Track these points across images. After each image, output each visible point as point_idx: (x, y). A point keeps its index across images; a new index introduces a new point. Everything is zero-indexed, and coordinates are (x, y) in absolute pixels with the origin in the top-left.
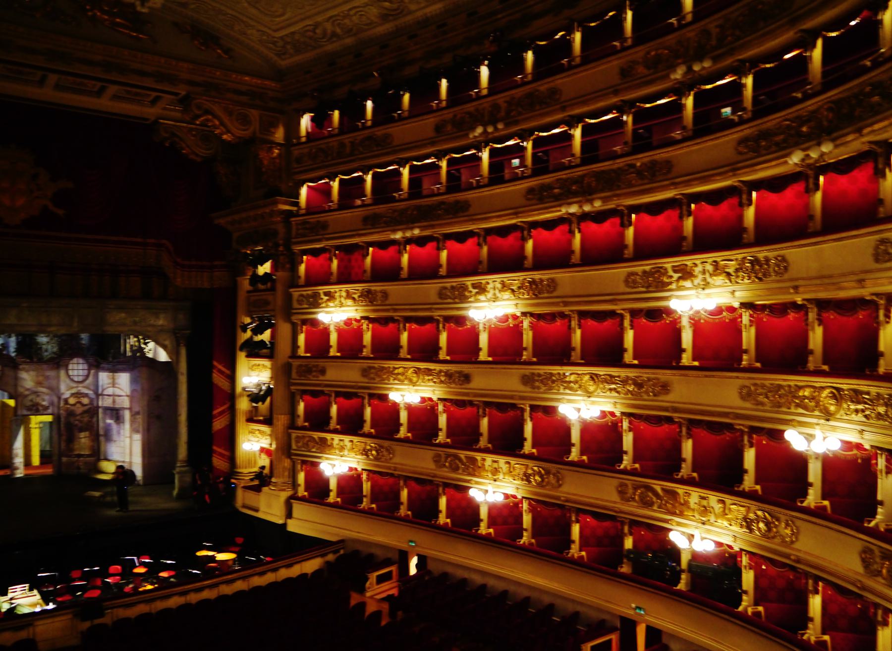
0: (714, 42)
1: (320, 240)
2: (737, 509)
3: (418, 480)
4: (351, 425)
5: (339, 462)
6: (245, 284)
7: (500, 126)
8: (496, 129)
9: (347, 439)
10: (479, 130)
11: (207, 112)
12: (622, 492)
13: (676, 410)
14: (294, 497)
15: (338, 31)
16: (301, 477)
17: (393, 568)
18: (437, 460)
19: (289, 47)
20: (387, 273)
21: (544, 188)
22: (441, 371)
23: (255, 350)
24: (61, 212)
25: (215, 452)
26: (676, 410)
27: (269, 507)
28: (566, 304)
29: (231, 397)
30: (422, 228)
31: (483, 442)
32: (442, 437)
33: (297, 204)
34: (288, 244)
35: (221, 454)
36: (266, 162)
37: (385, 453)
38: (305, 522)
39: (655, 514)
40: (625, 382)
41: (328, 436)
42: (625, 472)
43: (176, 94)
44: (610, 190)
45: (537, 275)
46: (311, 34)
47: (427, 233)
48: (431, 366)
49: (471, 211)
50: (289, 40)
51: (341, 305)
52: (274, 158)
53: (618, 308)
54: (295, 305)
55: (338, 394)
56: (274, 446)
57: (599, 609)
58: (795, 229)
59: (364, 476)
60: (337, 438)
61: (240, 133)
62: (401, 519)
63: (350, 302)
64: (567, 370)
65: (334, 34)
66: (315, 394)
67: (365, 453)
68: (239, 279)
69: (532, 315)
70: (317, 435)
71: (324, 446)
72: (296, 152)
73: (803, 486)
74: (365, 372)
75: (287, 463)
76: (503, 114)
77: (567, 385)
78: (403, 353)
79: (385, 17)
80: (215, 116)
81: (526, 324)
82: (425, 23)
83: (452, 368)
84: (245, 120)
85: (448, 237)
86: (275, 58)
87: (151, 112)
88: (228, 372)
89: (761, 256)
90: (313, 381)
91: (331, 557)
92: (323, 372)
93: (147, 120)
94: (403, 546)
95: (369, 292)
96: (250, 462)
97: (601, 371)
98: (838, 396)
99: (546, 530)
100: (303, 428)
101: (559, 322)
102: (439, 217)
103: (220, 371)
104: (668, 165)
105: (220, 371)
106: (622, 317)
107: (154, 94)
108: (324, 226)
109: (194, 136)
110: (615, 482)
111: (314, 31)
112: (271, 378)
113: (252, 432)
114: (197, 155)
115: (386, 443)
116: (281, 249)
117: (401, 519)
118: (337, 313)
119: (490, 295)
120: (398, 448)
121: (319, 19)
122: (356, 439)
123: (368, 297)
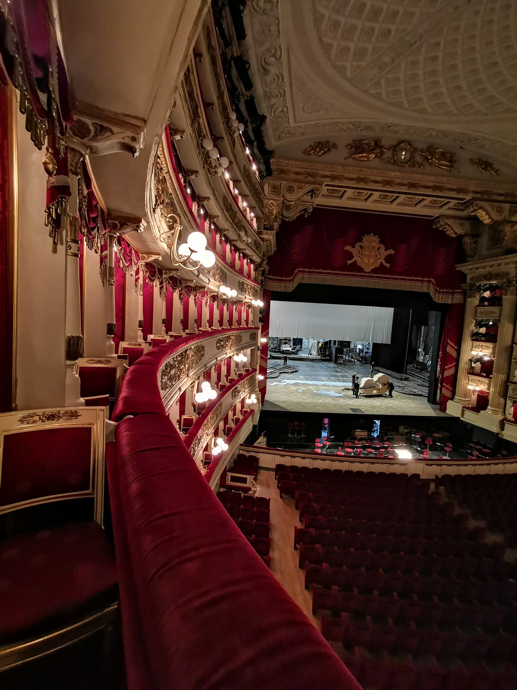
11: (481, 208)
14: (505, 419)
16: (510, 410)
23: (476, 337)
24: (388, 265)
25: (445, 387)
27: (487, 420)
29: (457, 360)
36: (508, 234)
43: (464, 199)
52: (514, 231)
56: (492, 390)
75: (502, 400)
84: (500, 211)
87: (434, 212)
88: (456, 348)
93: (432, 217)
96: (466, 394)
103: (452, 346)
105: (452, 346)
107: (447, 200)
109: (456, 223)
112: (493, 353)
113: (473, 381)
116: (514, 282)
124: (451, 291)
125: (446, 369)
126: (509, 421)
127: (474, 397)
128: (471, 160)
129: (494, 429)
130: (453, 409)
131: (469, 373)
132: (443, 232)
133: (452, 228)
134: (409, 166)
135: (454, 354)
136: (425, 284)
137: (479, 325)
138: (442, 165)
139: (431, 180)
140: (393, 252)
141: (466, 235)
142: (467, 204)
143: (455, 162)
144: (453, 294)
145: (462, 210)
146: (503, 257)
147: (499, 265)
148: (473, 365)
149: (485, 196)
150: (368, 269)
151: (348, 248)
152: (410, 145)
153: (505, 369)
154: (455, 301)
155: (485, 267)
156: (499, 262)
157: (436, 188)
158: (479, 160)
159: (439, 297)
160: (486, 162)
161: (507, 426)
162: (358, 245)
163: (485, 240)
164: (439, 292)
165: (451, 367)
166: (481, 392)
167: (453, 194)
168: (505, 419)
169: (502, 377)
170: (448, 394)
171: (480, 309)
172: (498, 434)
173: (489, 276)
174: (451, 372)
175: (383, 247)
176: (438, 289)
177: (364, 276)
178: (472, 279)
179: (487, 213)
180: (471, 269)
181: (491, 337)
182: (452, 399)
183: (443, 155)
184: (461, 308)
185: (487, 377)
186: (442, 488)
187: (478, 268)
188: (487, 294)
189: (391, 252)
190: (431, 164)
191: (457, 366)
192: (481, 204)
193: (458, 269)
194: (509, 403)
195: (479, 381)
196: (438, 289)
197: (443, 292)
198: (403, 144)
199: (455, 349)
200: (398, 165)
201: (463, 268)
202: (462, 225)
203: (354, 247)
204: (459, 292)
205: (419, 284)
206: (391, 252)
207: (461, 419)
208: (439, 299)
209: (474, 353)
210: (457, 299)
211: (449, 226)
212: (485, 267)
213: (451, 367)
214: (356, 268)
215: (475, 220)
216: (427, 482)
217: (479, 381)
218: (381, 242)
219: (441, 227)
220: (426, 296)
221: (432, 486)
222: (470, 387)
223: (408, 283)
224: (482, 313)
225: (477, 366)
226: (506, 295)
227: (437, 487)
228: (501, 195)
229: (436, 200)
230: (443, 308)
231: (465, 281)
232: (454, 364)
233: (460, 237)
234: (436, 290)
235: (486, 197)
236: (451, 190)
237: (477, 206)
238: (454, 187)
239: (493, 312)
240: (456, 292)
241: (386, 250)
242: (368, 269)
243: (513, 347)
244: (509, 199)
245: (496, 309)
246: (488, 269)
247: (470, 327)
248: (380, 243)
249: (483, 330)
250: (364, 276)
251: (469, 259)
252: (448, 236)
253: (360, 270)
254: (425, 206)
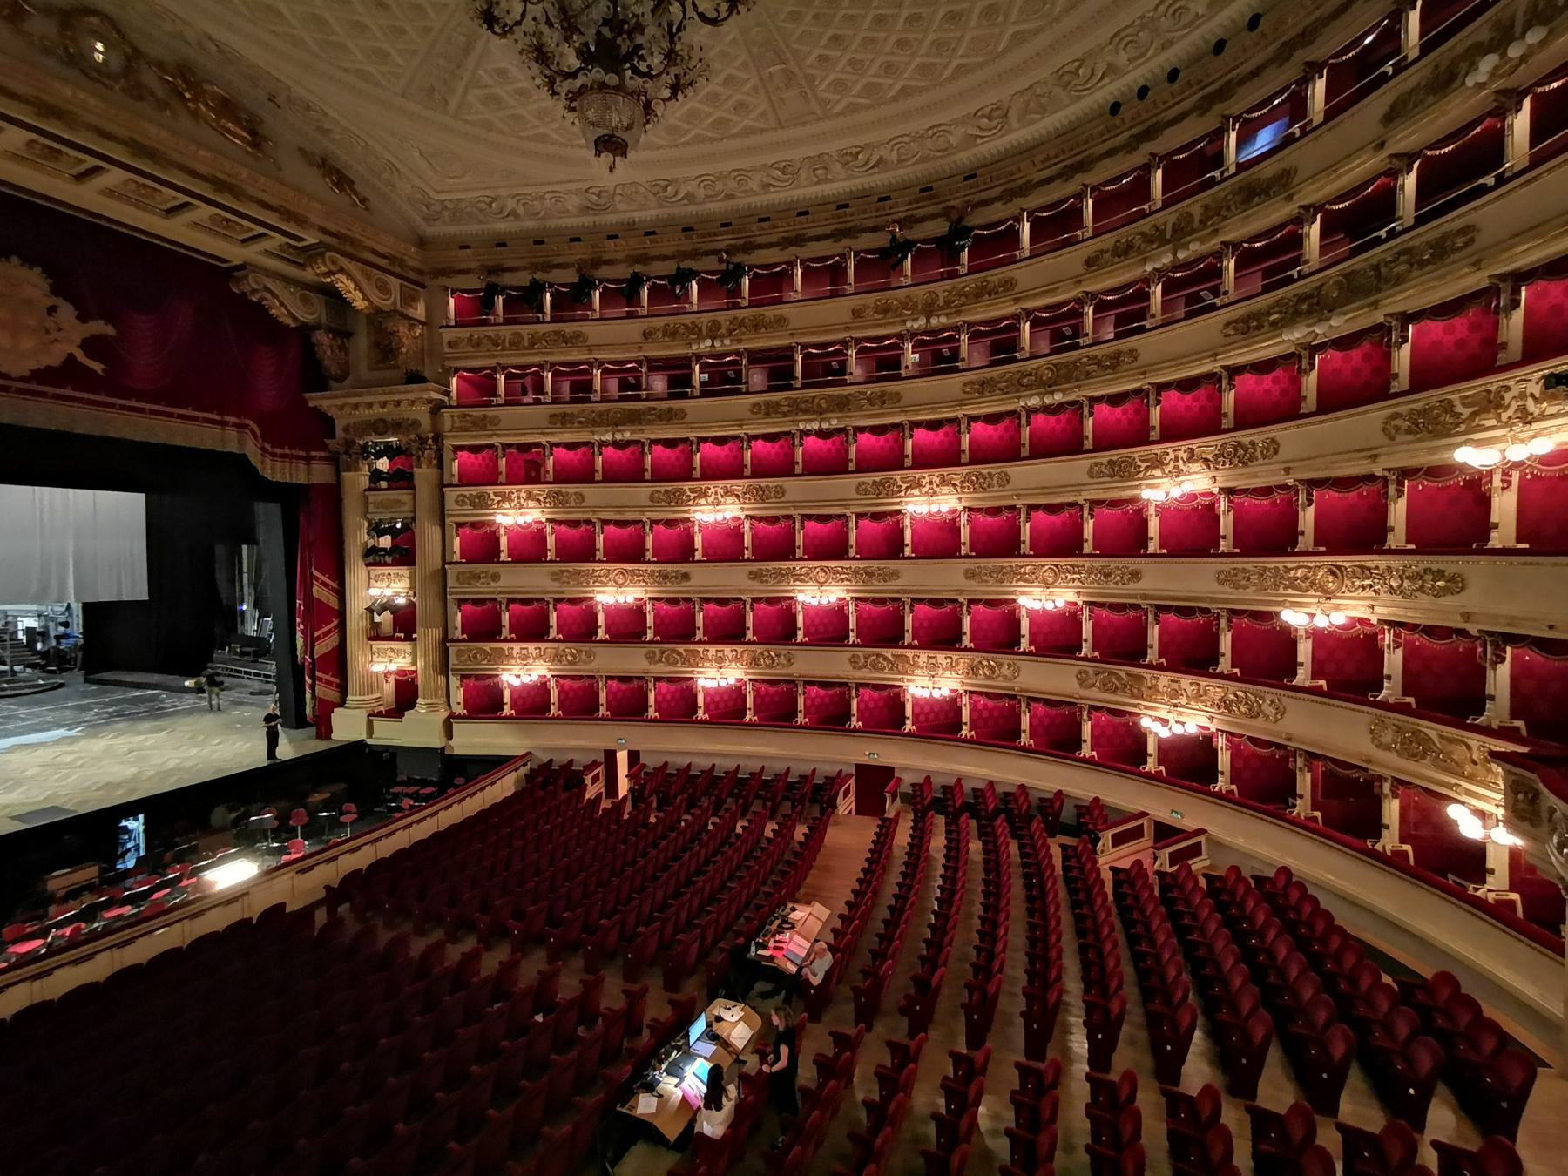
0: (941, 303)
1: (490, 436)
2: (963, 660)
3: (622, 679)
4: (532, 630)
5: (522, 670)
6: (357, 479)
7: (727, 342)
8: (723, 345)
9: (531, 647)
10: (708, 343)
11: (342, 270)
12: (853, 661)
13: (905, 592)
14: (452, 716)
15: (521, 210)
16: (458, 695)
17: (601, 769)
18: (650, 657)
19: (446, 213)
20: (584, 475)
21: (768, 404)
22: (653, 572)
23: (374, 557)
24: (98, 367)
25: (320, 680)
26: (905, 592)
27: (418, 730)
28: (795, 508)
29: (341, 614)
30: (633, 432)
31: (699, 635)
32: (650, 635)
33: (448, 394)
34: (438, 438)
35: (329, 683)
37: (583, 656)
38: (474, 739)
39: (887, 676)
40: (856, 572)
41: (505, 646)
42: (854, 645)
43: (302, 239)
44: (841, 411)
45: (764, 482)
46: (482, 205)
47: (636, 437)
48: (643, 567)
49: (687, 419)
50: (450, 206)
51: (521, 507)
53: (847, 512)
54: (450, 503)
55: (511, 601)
57: (834, 763)
58: (1008, 453)
59: (552, 683)
60: (517, 647)
61: (377, 302)
62: (603, 719)
63: (532, 504)
64: (798, 565)
65: (513, 213)
66: (476, 602)
67: (557, 658)
68: (347, 476)
69: (752, 517)
70: (487, 646)
71: (501, 657)
72: (448, 335)
73: (1017, 637)
74: (556, 576)
75: (442, 679)
76: (723, 331)
77: (798, 578)
78: (599, 555)
79: (586, 210)
80: (350, 276)
81: (747, 526)
82: (630, 227)
83: (669, 567)
84: (384, 289)
85: (654, 442)
86: (419, 220)
87: (234, 253)
88: (334, 585)
89: (985, 472)
90: (482, 589)
91: (523, 771)
92: (496, 577)
93: (225, 261)
94: (611, 746)
95: (558, 493)
96: (372, 684)
97: (832, 564)
98: (1056, 570)
99: (776, 707)
100: (463, 641)
101: (783, 523)
102: (650, 422)
103: (323, 583)
104: (897, 396)
105: (323, 583)
106: (847, 518)
108: (494, 421)
110: (849, 655)
111: (490, 205)
112: (412, 587)
113: (381, 653)
114: (295, 318)
115: (586, 647)
117: (603, 719)
118: (517, 514)
119: (710, 500)
120: (600, 650)
121: (503, 192)
122: (543, 646)
123: (557, 500)
124: (302, 453)
125: (319, 638)
126: (459, 717)
127: (389, 688)
128: (300, 149)
129: (435, 741)
130: (348, 726)
131: (370, 639)
132: (260, 310)
133: (282, 304)
134: (123, 90)
135: (333, 602)
136: (232, 433)
137: (377, 530)
138: (228, 131)
139: (203, 160)
140: (110, 330)
141: (318, 326)
142: (309, 255)
143: (266, 139)
144: (308, 459)
145: (301, 266)
146: (402, 388)
147: (398, 403)
148: (377, 619)
149: (344, 245)
152: (119, 32)
153: (438, 619)
154: (315, 480)
155: (370, 405)
156: (397, 397)
157: (221, 185)
158: (324, 160)
159: (273, 468)
160: (338, 172)
161: (457, 727)
163: (362, 343)
164: (273, 455)
165: (326, 634)
166: (401, 672)
167: (271, 218)
168: (452, 716)
169: (436, 633)
170: (331, 694)
171: (374, 497)
172: (443, 749)
173: (381, 426)
174: (330, 643)
176: (268, 446)
178: (346, 429)
179: (358, 287)
180: (341, 408)
181: (403, 555)
182: (342, 704)
183: (227, 107)
184: (332, 496)
185: (409, 638)
186: (344, 909)
187: (356, 406)
188: (383, 464)
190: (195, 114)
191: (342, 627)
192: (344, 262)
193: (311, 404)
194: (454, 682)
195: (392, 650)
196: (268, 446)
197: (283, 456)
198: (94, 20)
199: (333, 590)
200: (84, 72)
201: (320, 401)
202: (305, 300)
204: (321, 458)
205: (217, 431)
207: (369, 741)
208: (274, 470)
209: (374, 592)
210: (320, 473)
211: (273, 294)
212: (370, 405)
213: (326, 634)
215: (334, 296)
216: (307, 913)
217: (392, 650)
219: (254, 291)
221: (321, 916)
222: (378, 667)
223: (178, 425)
224: (380, 505)
225: (385, 619)
226: (419, 466)
227: (332, 912)
228: (383, 256)
229: (229, 220)
230: (290, 497)
231: (333, 436)
232: (335, 622)
233: (305, 330)
234: (263, 449)
235: (348, 248)
236: (266, 206)
237: (333, 263)
238: (274, 202)
239: (400, 503)
240: (314, 458)
243: (445, 571)
244: (397, 269)
245: (404, 496)
246: (378, 411)
247: (358, 537)
249: (385, 542)
251: (332, 383)
252: (274, 321)
254: (196, 225)
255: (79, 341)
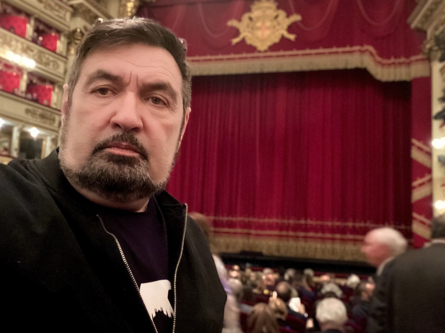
25: (416, 219)
125: (414, 188)
144: (409, 64)
150: (262, 46)
151: (233, 23)
162: (245, 17)
175: (282, 14)
177: (258, 57)
189: (296, 18)
203: (240, 20)
204: (417, 60)
206: (296, 18)
214: (246, 48)
218: (278, 8)
220: (361, 74)
241: (288, 16)
242: (262, 46)
248: (278, 8)
250: (258, 57)
253: (252, 49)
255: (285, 26)
